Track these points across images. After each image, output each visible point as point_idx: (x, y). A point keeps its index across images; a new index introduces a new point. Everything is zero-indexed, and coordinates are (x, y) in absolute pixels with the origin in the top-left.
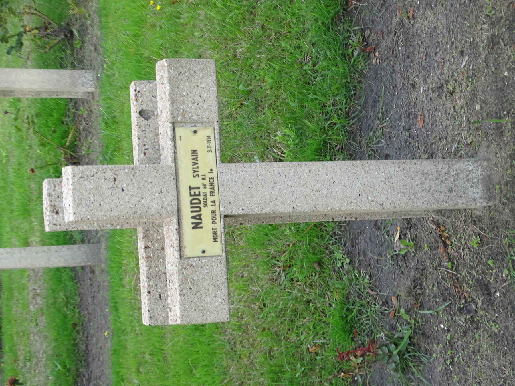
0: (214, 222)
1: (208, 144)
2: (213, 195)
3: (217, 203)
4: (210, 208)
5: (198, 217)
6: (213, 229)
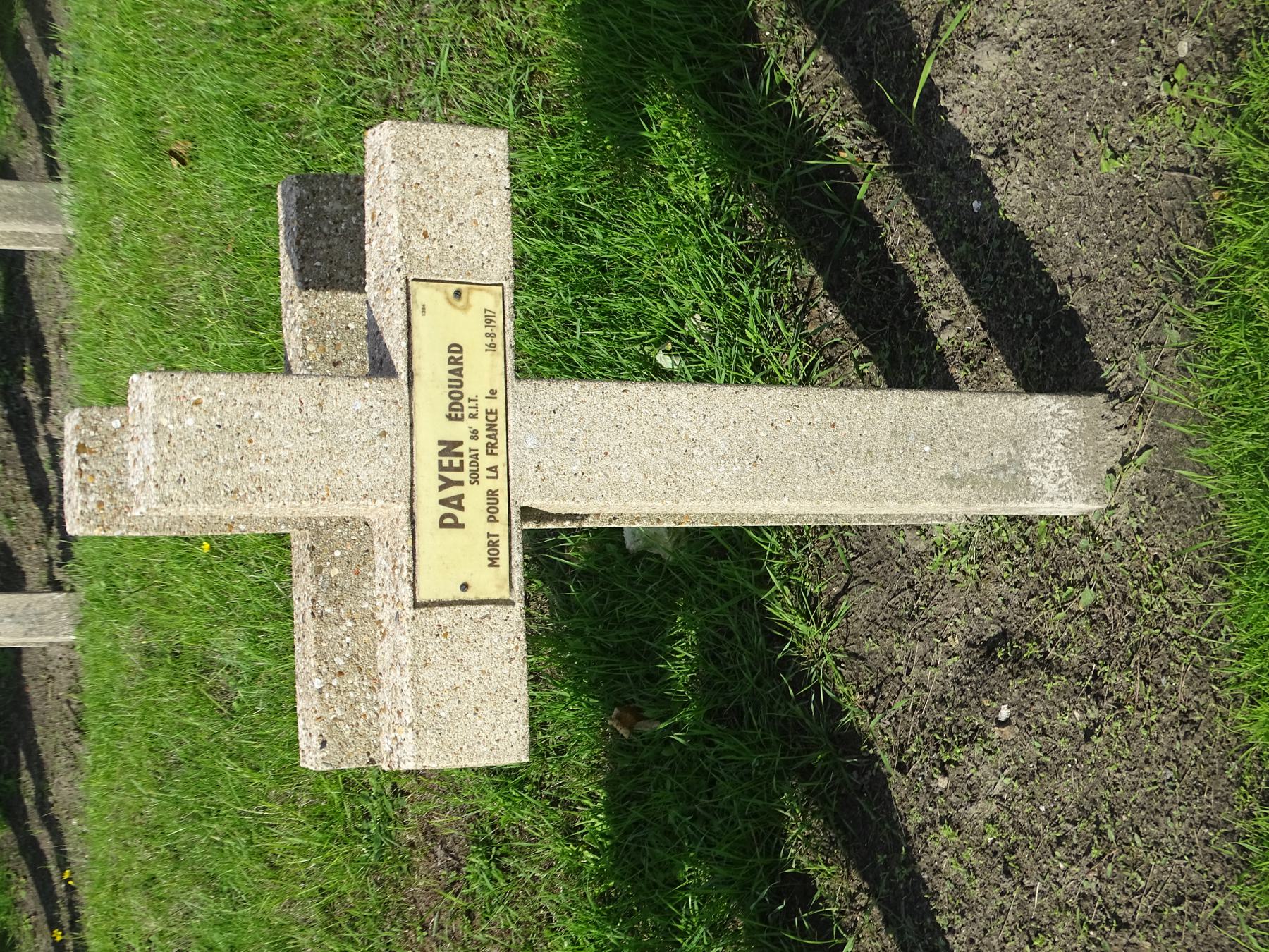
0: (492, 519)
1: (489, 330)
2: (492, 454)
3: (502, 471)
4: (486, 484)
5: (455, 503)
6: (489, 535)
